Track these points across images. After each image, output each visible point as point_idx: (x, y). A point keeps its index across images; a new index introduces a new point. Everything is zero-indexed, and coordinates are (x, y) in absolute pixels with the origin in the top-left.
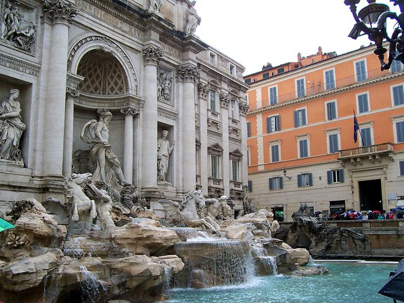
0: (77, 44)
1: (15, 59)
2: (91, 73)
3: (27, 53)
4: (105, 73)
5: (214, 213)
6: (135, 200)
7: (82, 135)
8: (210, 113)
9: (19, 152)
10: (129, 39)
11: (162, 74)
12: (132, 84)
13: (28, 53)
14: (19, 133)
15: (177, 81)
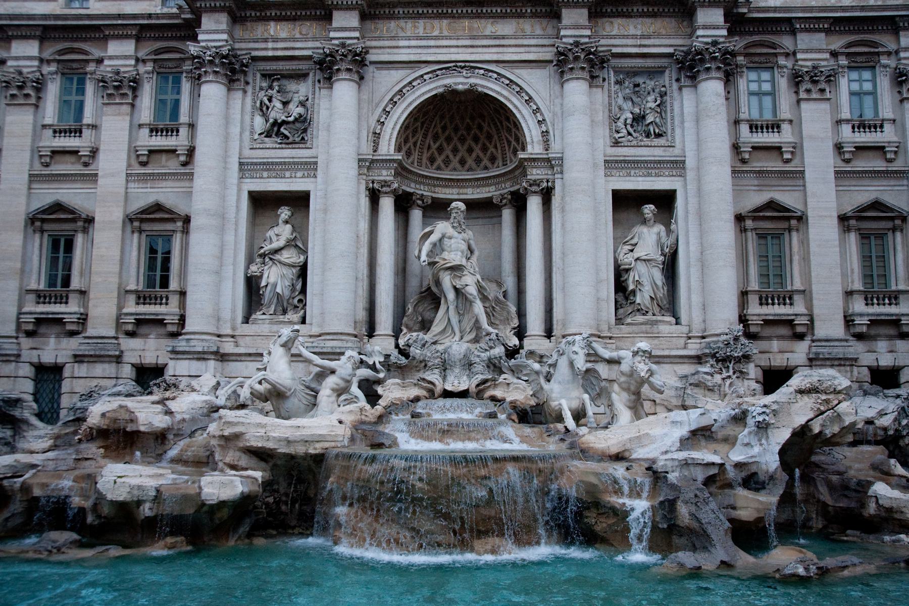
0: (391, 100)
1: (272, 163)
2: (476, 134)
3: (297, 146)
4: (496, 126)
5: (624, 386)
6: (494, 366)
7: (416, 253)
8: (846, 129)
9: (300, 301)
10: (516, 46)
11: (638, 85)
12: (531, 131)
13: (301, 146)
14: (291, 273)
15: (680, 89)
